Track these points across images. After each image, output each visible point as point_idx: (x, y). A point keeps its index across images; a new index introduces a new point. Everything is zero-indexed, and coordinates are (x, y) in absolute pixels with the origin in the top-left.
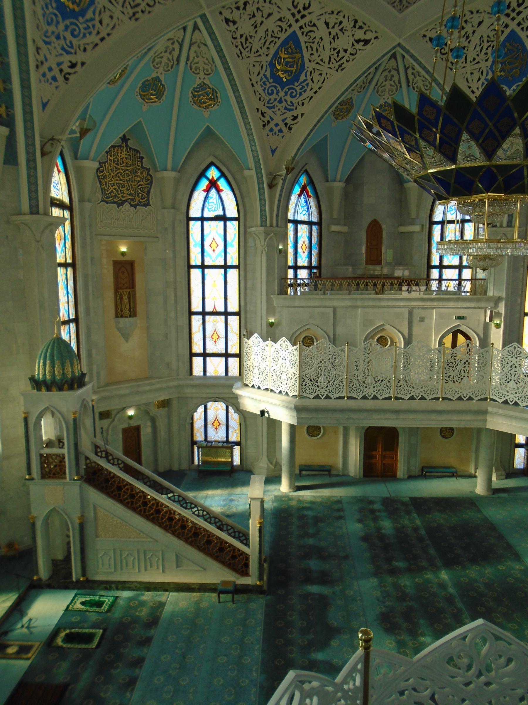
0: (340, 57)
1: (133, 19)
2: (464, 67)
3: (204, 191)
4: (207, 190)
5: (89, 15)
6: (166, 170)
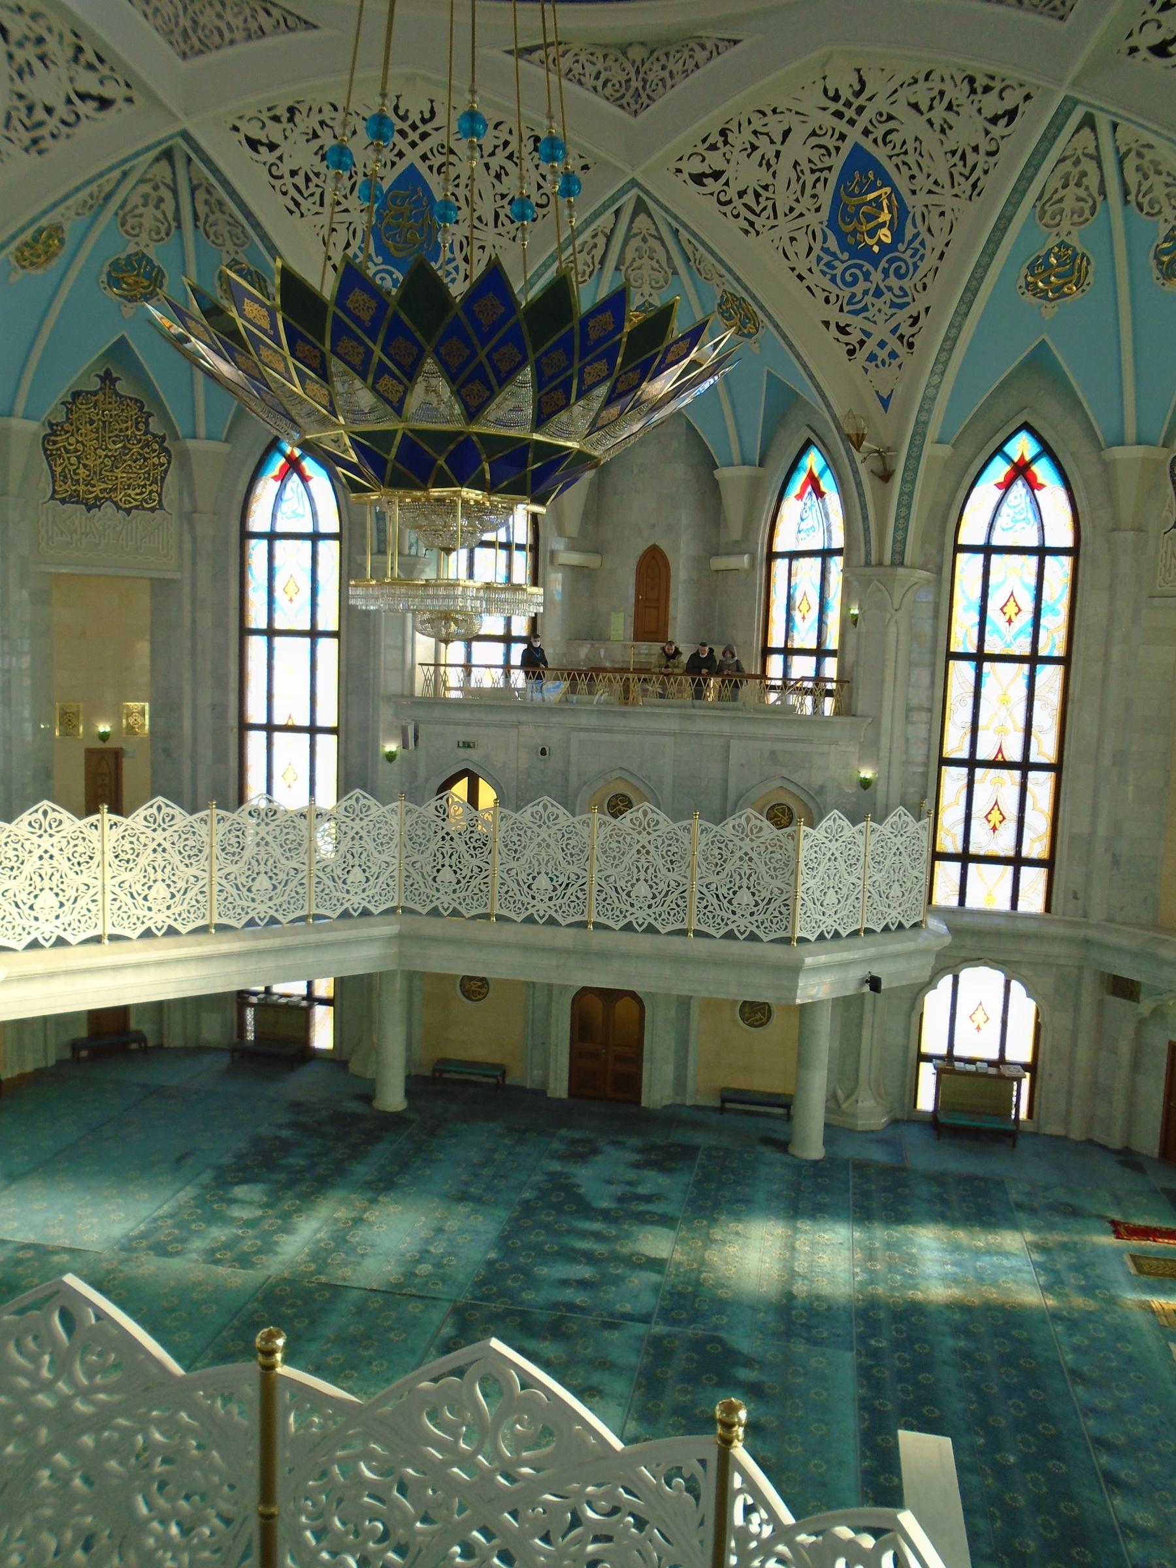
2: (773, 227)
4: (283, 477)
6: (195, 437)
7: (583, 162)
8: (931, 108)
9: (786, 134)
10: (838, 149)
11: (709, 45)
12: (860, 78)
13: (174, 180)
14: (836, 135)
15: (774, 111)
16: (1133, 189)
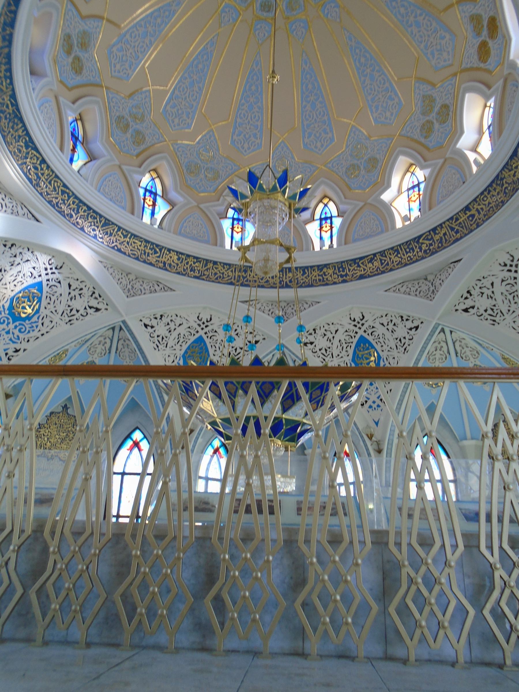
0: (237, 352)
1: (69, 324)
3: (128, 450)
4: (131, 449)
5: (35, 319)
7: (263, 337)
8: (388, 325)
9: (336, 331)
10: (355, 337)
11: (309, 303)
12: (363, 315)
13: (113, 337)
14: (354, 332)
15: (333, 324)
16: (459, 352)
